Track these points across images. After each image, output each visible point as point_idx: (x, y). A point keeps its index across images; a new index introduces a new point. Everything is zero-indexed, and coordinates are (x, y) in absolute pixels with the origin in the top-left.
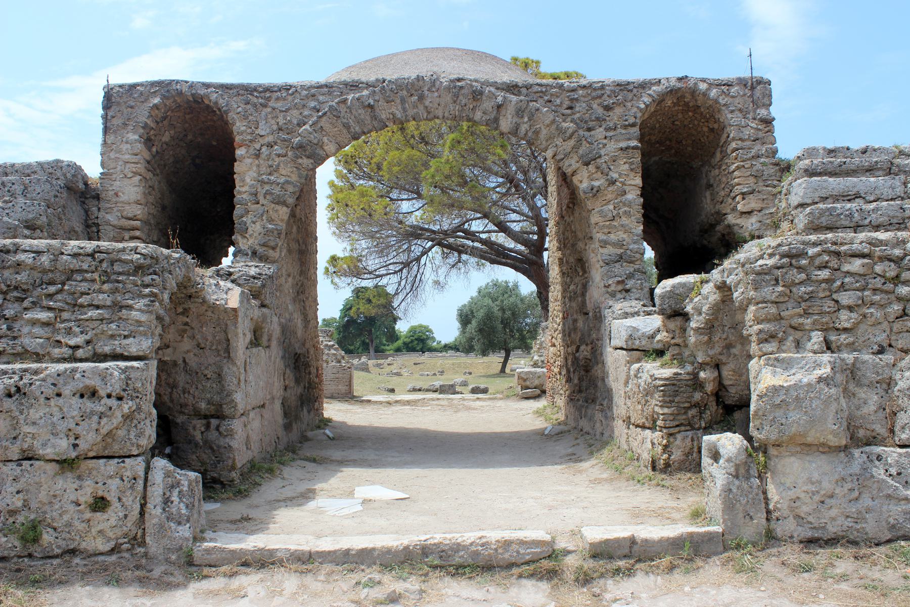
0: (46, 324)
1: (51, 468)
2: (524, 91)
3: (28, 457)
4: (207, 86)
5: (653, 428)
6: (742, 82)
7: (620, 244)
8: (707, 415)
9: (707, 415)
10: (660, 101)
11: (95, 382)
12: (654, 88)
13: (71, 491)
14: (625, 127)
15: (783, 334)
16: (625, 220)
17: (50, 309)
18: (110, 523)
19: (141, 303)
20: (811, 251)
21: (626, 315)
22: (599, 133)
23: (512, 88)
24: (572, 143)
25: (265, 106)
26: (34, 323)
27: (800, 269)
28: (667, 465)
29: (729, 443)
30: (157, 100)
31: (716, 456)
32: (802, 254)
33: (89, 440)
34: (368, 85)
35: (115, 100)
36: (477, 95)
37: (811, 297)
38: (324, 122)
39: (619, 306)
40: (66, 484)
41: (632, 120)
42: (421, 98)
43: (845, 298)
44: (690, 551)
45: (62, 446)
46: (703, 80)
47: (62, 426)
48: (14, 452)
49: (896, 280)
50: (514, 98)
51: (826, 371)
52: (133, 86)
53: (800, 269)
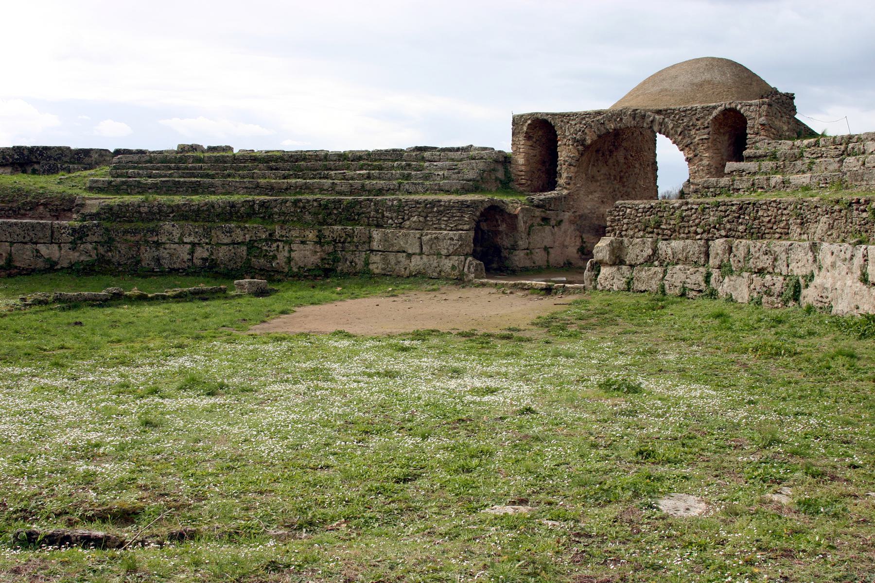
4: (547, 114)
14: (704, 129)
19: (467, 216)
22: (693, 132)
23: (659, 112)
30: (529, 122)
33: (451, 251)
35: (517, 121)
36: (643, 117)
37: (619, 220)
40: (447, 261)
41: (706, 125)
42: (621, 119)
43: (625, 221)
50: (657, 117)
52: (522, 116)
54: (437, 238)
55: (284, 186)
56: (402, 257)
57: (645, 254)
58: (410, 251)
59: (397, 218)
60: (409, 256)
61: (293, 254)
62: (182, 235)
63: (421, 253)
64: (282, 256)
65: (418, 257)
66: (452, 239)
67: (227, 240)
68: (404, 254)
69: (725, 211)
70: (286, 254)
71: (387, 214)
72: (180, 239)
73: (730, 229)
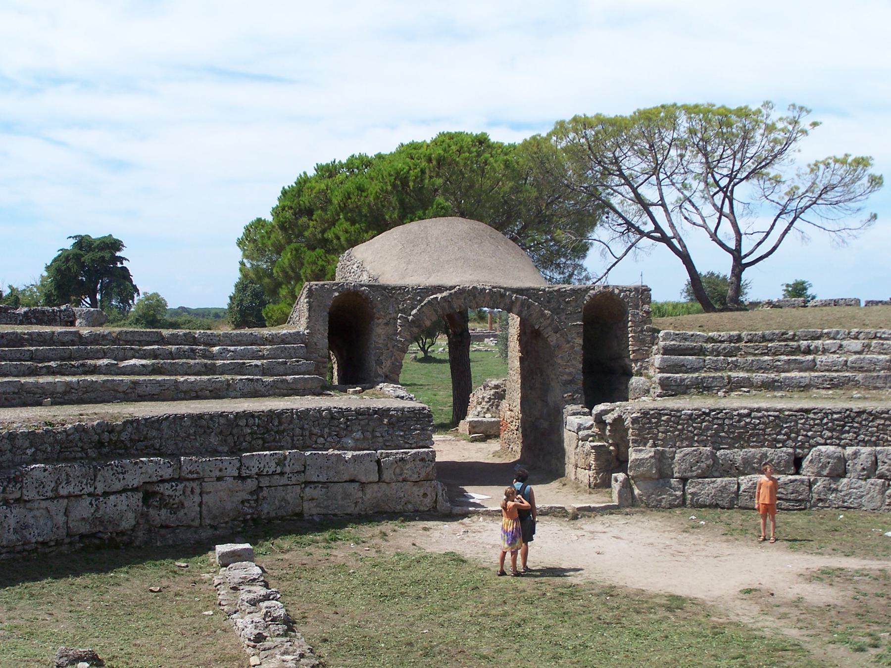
0: (401, 436)
1: (412, 484)
2: (525, 293)
3: (404, 480)
5: (589, 470)
6: (636, 289)
7: (570, 374)
8: (612, 465)
9: (612, 465)
10: (594, 298)
11: (425, 456)
12: (591, 291)
13: (417, 491)
15: (641, 441)
16: (574, 362)
17: (402, 431)
18: (428, 501)
20: (652, 412)
21: (574, 414)
24: (549, 321)
25: (391, 297)
26: (397, 436)
27: (648, 418)
28: (595, 485)
29: (621, 476)
30: (337, 294)
31: (617, 481)
32: (648, 413)
33: (423, 475)
34: (446, 289)
36: (503, 296)
38: (424, 309)
39: (570, 408)
43: (661, 429)
44: (609, 510)
45: (415, 477)
46: (617, 287)
47: (415, 471)
48: (401, 479)
49: (678, 424)
51: (652, 454)
53: (648, 418)
54: (402, 459)
55: (60, 389)
56: (353, 488)
57: (703, 465)
58: (364, 480)
59: (330, 435)
60: (363, 484)
61: (206, 498)
62: (58, 483)
63: (380, 480)
64: (192, 503)
65: (376, 487)
66: (423, 460)
67: (118, 486)
68: (356, 485)
69: (821, 420)
70: (197, 499)
71: (316, 430)
72: (55, 490)
73: (831, 438)
